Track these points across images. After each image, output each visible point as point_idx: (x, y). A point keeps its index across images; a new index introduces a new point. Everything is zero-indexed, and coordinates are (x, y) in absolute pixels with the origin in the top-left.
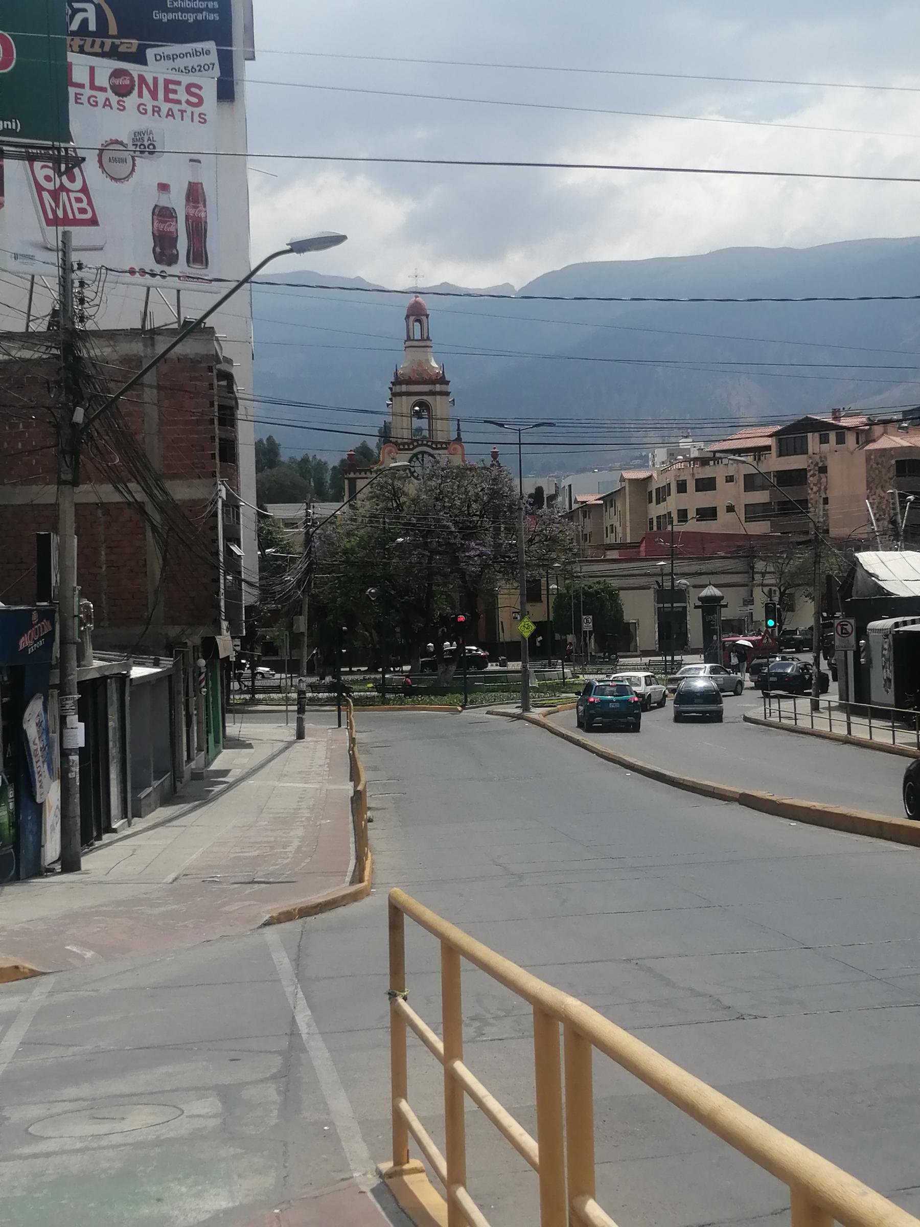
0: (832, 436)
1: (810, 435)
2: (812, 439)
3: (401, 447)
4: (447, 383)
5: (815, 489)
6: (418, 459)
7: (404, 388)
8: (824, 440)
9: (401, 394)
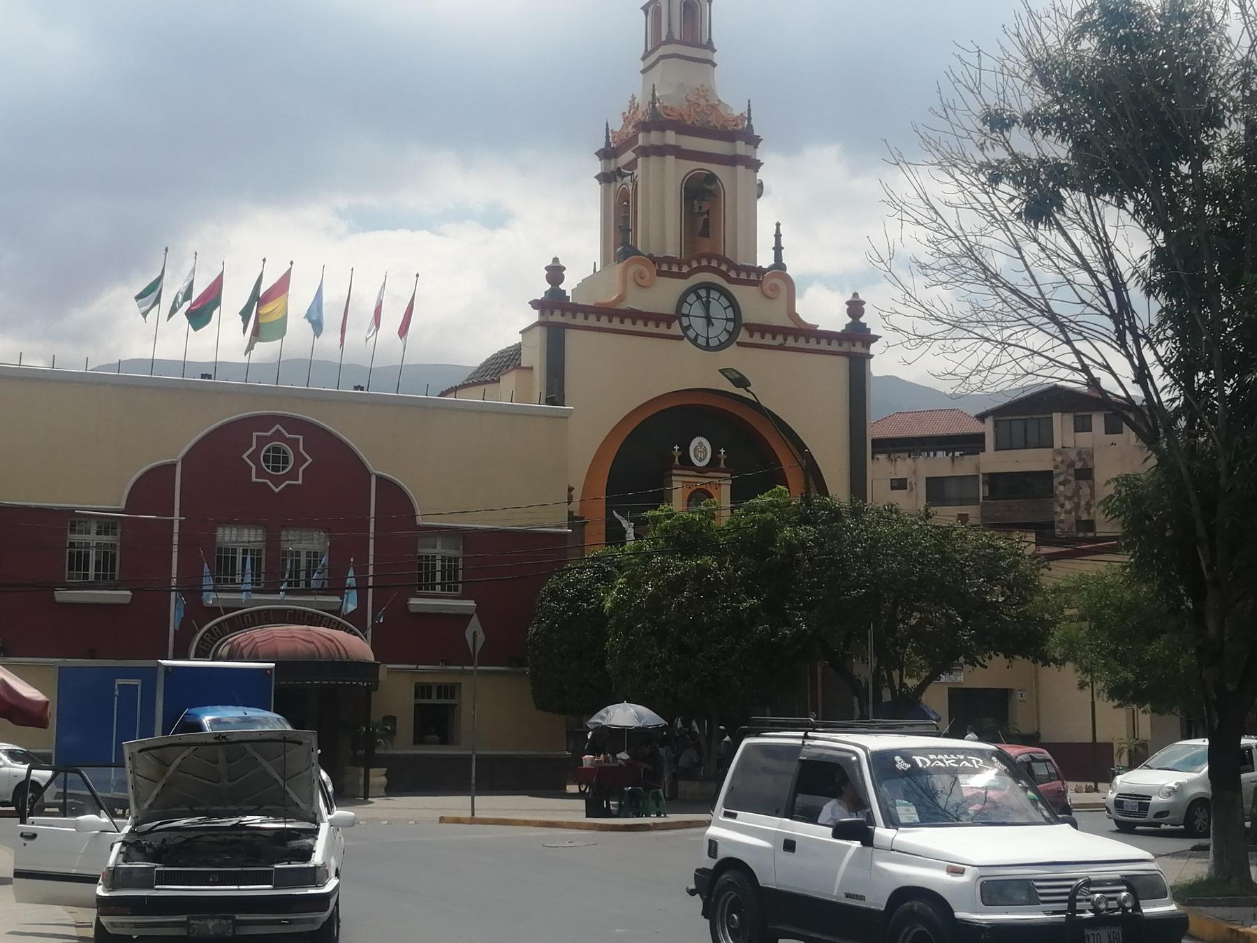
0: (1098, 421)
1: (1057, 417)
2: (1061, 424)
3: (665, 268)
5: (1068, 506)
6: (699, 297)
7: (671, 138)
8: (1083, 426)
9: (661, 151)
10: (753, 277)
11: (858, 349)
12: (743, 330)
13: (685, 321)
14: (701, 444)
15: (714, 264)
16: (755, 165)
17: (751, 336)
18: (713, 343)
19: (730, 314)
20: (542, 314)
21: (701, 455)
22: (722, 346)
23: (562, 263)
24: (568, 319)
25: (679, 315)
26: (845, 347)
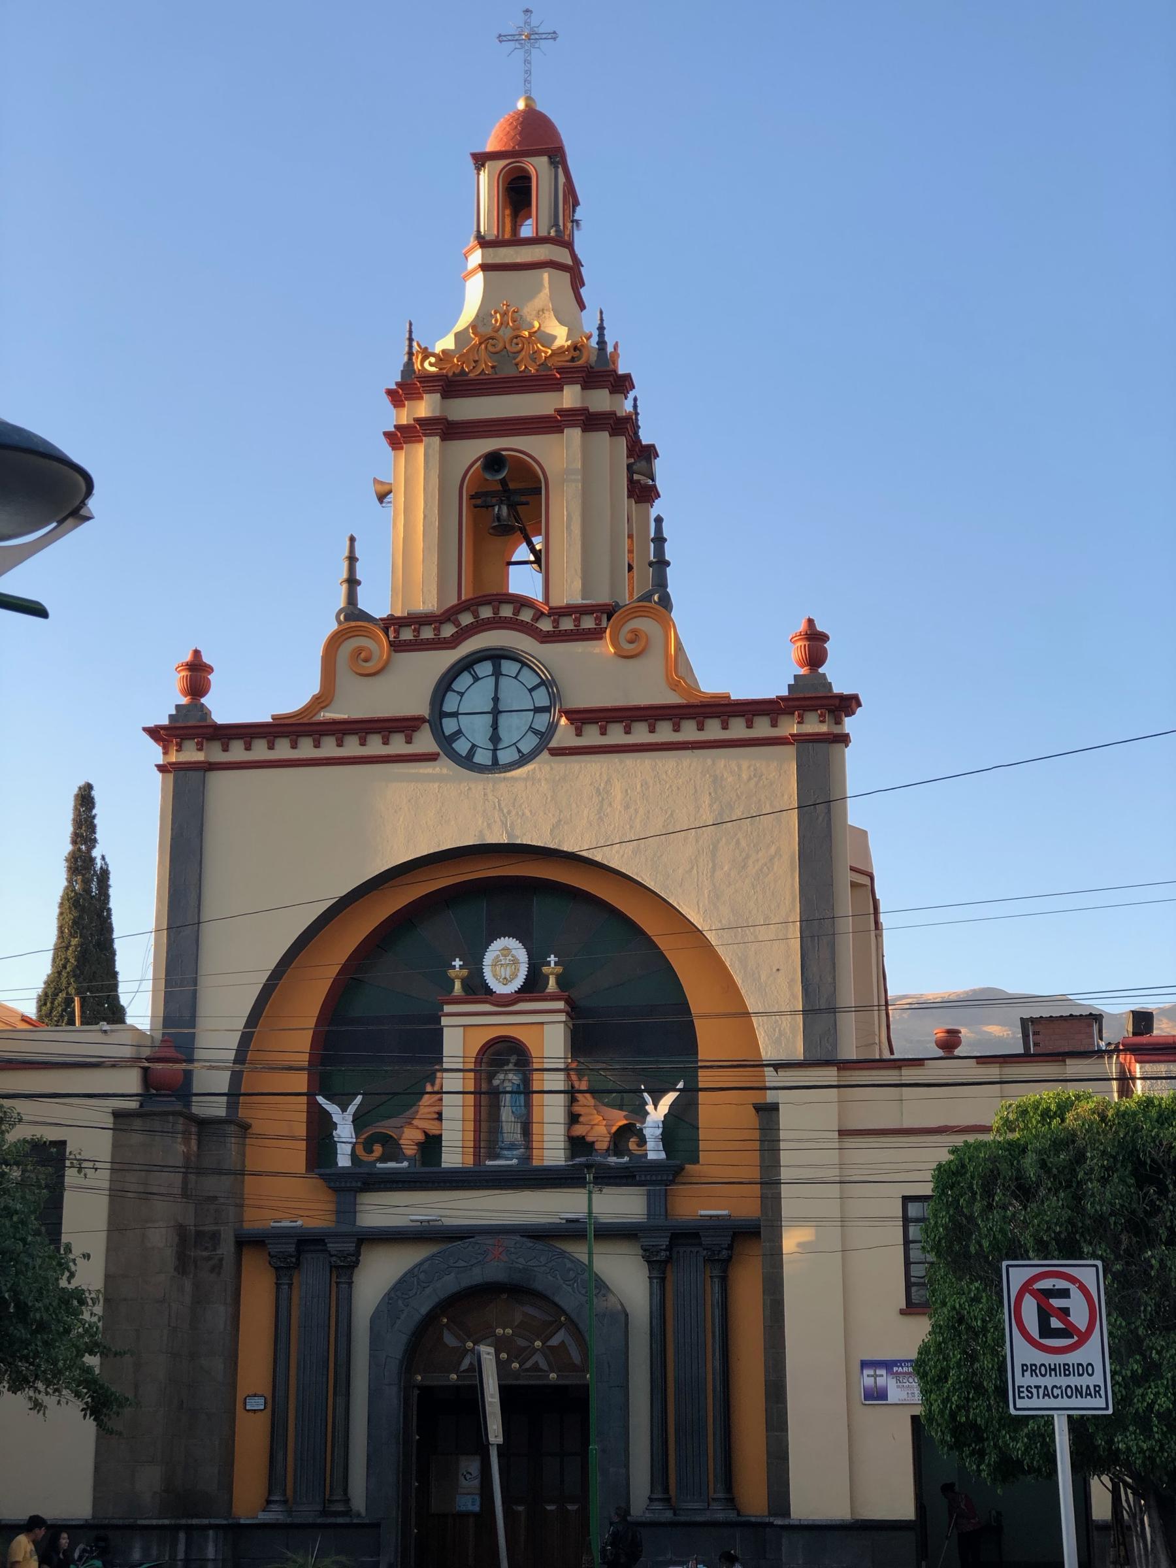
3: (407, 634)
4: (622, 384)
10: (588, 623)
13: (449, 726)
14: (506, 950)
15: (507, 611)
16: (624, 426)
17: (579, 733)
18: (505, 757)
20: (165, 753)
21: (506, 972)
22: (524, 759)
23: (206, 659)
24: (217, 755)
25: (438, 713)
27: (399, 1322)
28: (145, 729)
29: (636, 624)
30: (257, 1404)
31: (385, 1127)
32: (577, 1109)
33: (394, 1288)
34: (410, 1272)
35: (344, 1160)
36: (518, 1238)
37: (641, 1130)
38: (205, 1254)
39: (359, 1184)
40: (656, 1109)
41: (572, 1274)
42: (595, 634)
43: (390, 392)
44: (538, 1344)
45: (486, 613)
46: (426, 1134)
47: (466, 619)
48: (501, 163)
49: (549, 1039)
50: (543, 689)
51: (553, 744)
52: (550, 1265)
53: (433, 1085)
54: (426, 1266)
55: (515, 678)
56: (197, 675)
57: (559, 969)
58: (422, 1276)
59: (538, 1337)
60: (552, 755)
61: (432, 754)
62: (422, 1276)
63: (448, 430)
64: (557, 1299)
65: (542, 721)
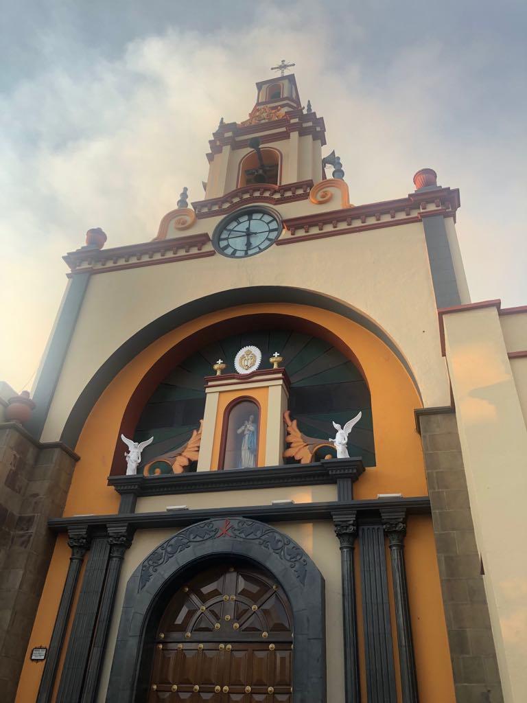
10: (300, 192)
11: (432, 207)
12: (284, 231)
13: (223, 244)
14: (249, 353)
15: (257, 194)
16: (320, 137)
17: (292, 234)
18: (250, 252)
19: (274, 225)
22: (261, 250)
26: (415, 214)
27: (148, 584)
28: (64, 258)
29: (324, 190)
30: (40, 655)
31: (165, 458)
32: (290, 439)
33: (148, 559)
34: (161, 546)
35: (131, 471)
36: (241, 518)
37: (333, 443)
38: (22, 532)
39: (136, 487)
40: (342, 428)
41: (280, 544)
42: (305, 196)
43: (210, 142)
44: (255, 607)
45: (247, 196)
46: (189, 460)
47: (236, 200)
48: (268, 85)
49: (272, 398)
50: (275, 222)
51: (280, 238)
52: (263, 538)
53: (198, 431)
54: (172, 542)
55: (260, 220)
56: (97, 236)
57: (280, 359)
58: (169, 549)
59: (255, 603)
60: (277, 245)
61: (211, 251)
62: (169, 549)
63: (236, 146)
64: (268, 564)
65: (273, 235)
